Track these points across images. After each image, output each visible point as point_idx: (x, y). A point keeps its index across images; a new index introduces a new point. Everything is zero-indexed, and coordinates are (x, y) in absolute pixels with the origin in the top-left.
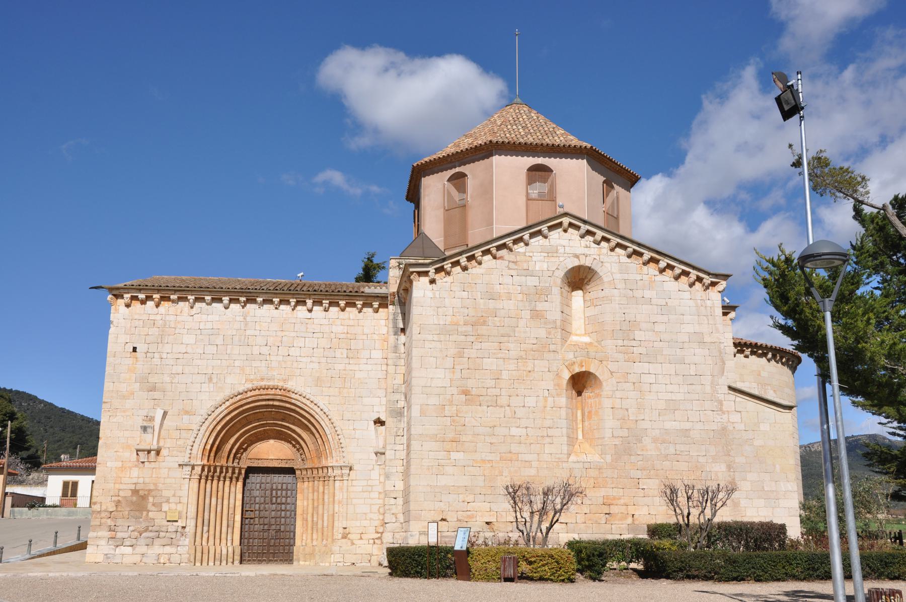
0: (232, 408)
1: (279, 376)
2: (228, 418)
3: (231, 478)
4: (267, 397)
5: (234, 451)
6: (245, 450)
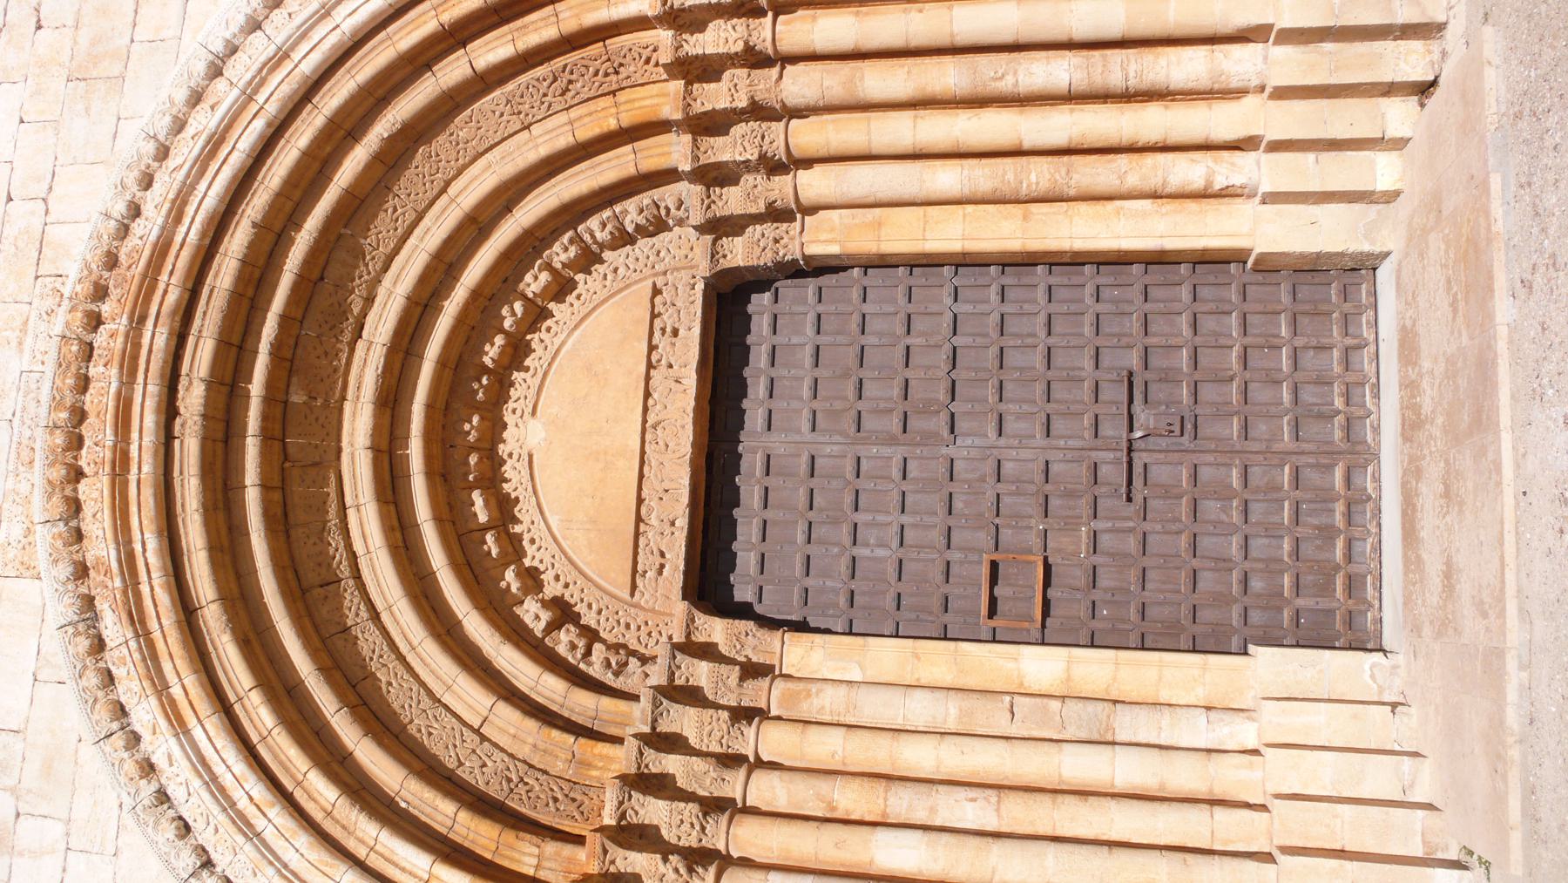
0: (184, 682)
1: (29, 341)
2: (259, 715)
3: (744, 715)
4: (146, 420)
5: (548, 688)
6: (563, 613)
